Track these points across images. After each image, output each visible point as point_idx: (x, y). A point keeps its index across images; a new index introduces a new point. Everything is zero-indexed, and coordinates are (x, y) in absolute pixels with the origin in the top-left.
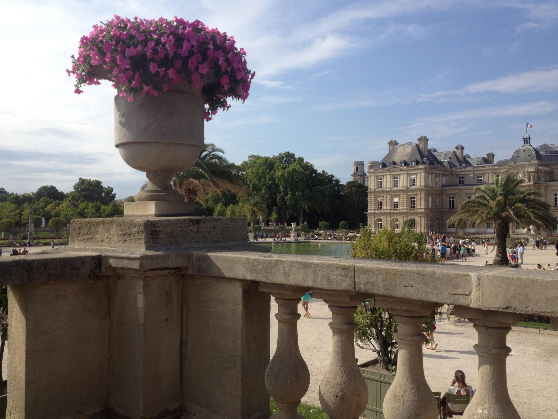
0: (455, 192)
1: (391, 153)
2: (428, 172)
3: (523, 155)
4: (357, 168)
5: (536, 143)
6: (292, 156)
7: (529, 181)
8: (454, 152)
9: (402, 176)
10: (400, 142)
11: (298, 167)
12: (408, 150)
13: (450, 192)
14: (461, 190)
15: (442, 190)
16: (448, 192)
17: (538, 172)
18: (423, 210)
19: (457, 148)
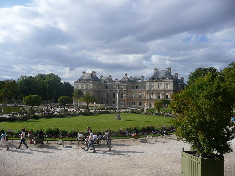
0: (104, 91)
1: (83, 76)
2: (94, 84)
7: (125, 89)
12: (88, 75)
13: (102, 91)
14: (105, 91)
15: (100, 90)
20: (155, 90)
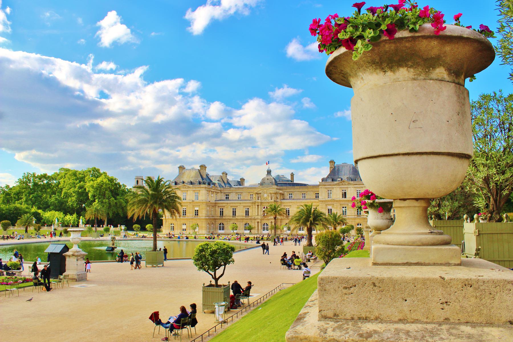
0: (224, 205)
3: (266, 181)
4: (137, 181)
5: (274, 174)
6: (98, 171)
8: (221, 177)
9: (189, 192)
10: (187, 167)
11: (105, 180)
12: (193, 174)
14: (228, 203)
15: (215, 203)
16: (219, 205)
17: (276, 193)
18: (204, 217)
19: (223, 173)
20: (337, 201)
